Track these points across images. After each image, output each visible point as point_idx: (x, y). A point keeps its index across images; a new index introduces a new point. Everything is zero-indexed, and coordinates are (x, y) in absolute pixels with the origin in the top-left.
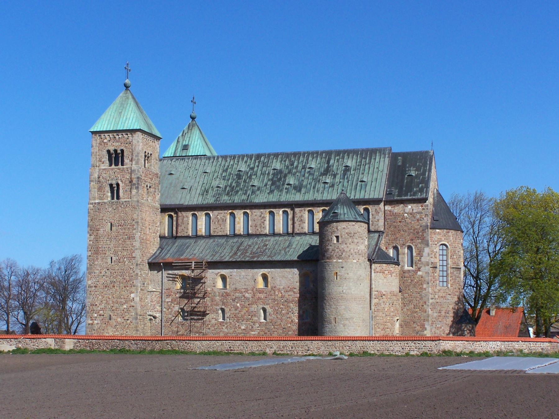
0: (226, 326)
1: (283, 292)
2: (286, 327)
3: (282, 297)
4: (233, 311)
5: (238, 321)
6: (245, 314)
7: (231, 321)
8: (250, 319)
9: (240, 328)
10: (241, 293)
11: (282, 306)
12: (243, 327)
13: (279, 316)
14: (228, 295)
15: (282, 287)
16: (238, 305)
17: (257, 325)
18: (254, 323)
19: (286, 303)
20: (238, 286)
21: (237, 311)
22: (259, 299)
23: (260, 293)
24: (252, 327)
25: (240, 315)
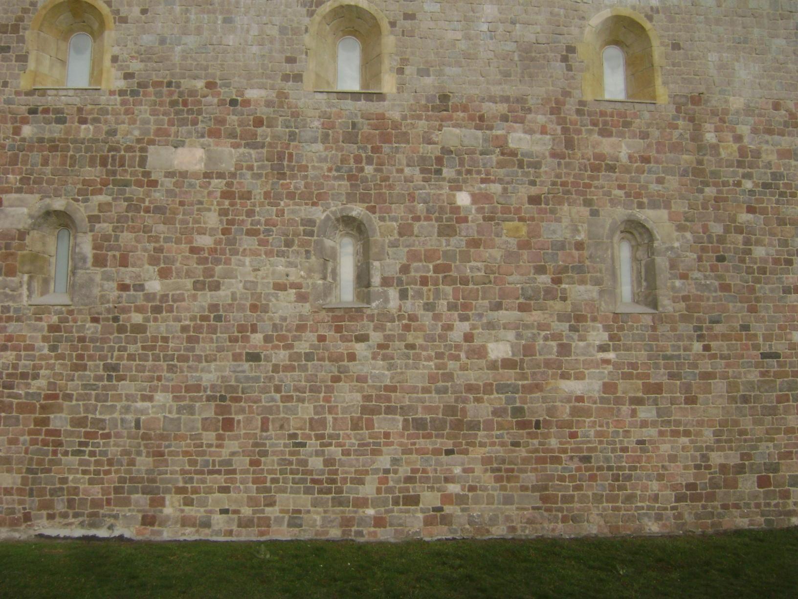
0: (376, 337)
1: (744, 130)
2: (779, 346)
3: (746, 159)
4: (427, 237)
5: (463, 309)
6: (510, 256)
7: (409, 306)
8: (549, 294)
9: (481, 352)
10: (481, 122)
11: (744, 217)
12: (498, 350)
13: (734, 280)
14: (386, 132)
15: (736, 103)
16: (463, 199)
17: (598, 335)
18: (577, 320)
19: (770, 202)
20: (462, 83)
21: (457, 243)
22: (603, 165)
23: (605, 133)
24: (565, 350)
25: (473, 268)
